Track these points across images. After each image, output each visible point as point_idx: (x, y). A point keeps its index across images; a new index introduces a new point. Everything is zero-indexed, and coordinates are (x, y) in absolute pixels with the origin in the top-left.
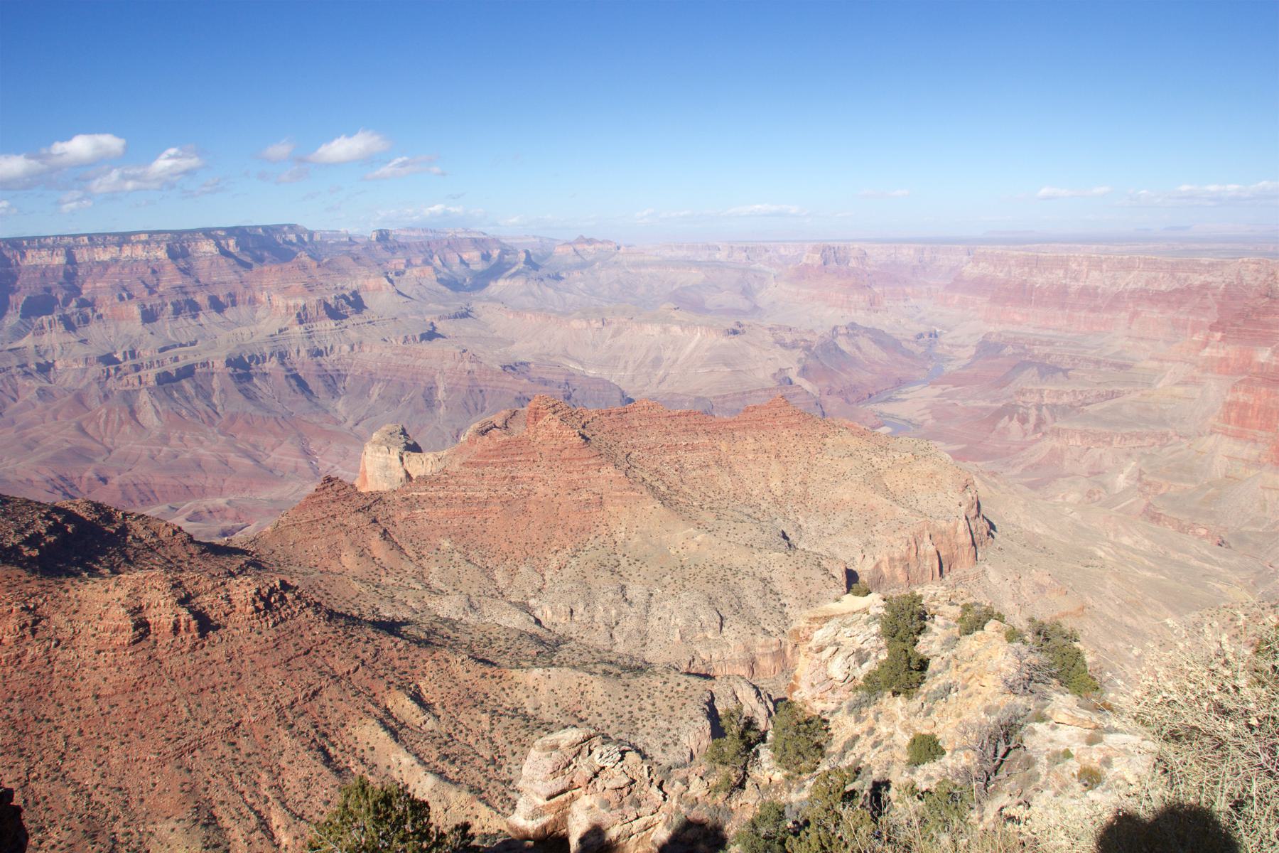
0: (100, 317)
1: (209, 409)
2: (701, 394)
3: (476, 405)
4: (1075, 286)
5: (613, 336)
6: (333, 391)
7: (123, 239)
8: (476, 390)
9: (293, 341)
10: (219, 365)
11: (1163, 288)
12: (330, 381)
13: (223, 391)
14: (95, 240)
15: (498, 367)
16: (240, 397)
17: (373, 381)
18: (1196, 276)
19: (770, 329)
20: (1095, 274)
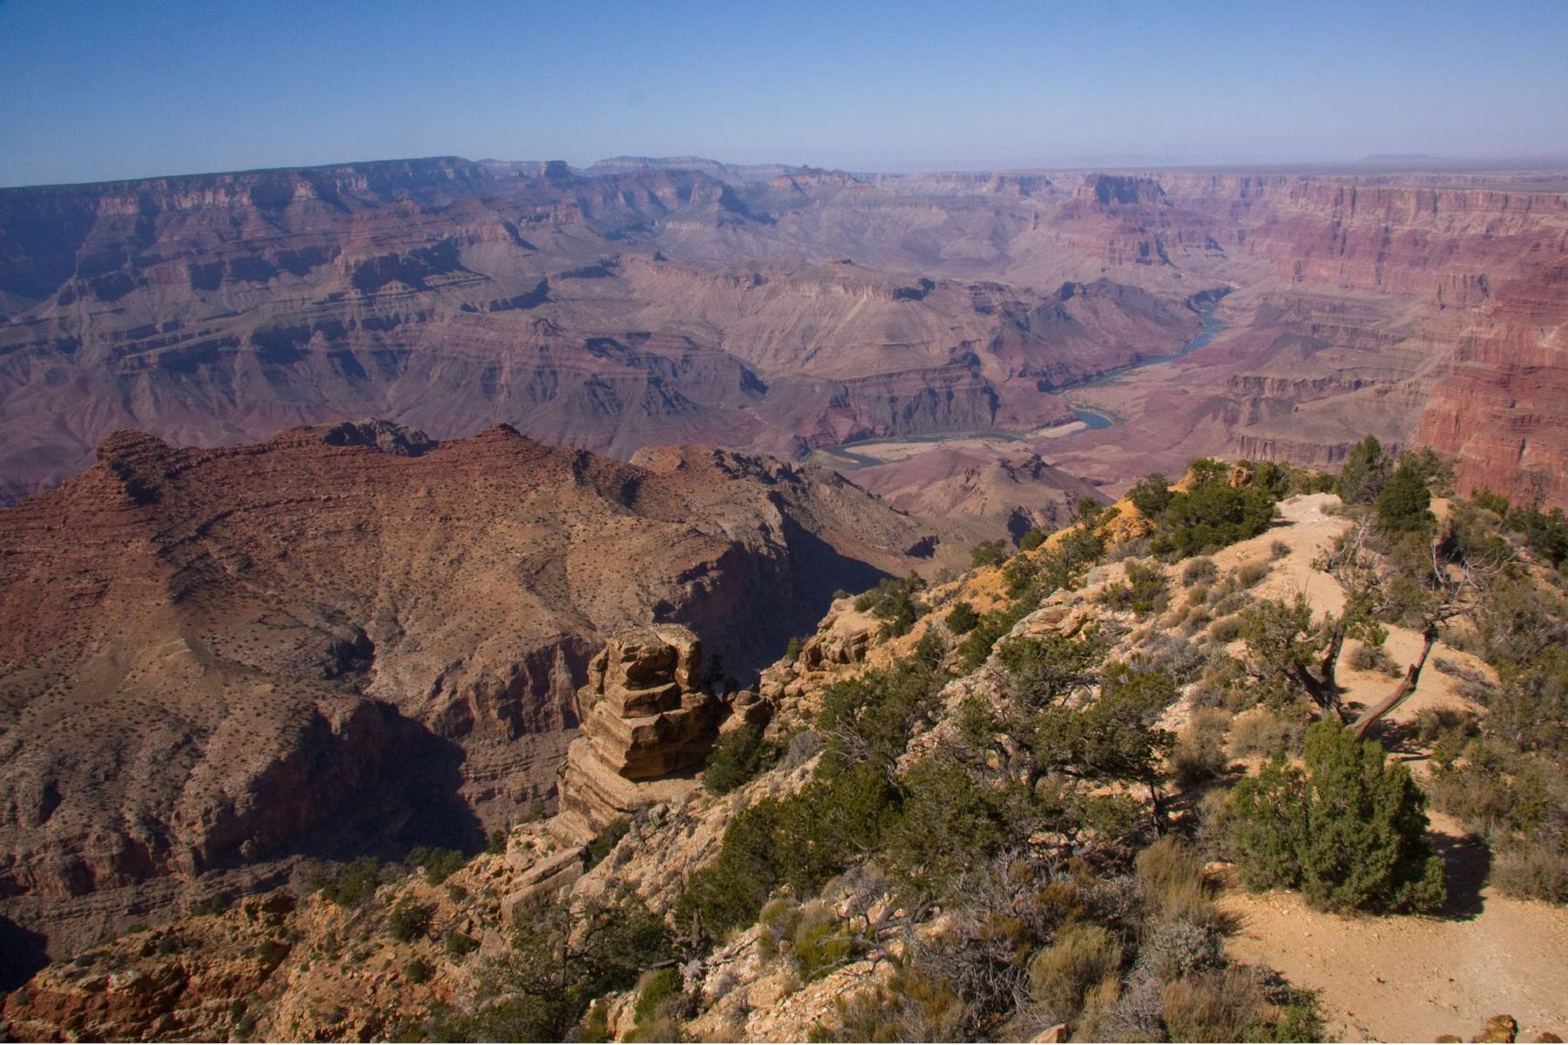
0: (144, 282)
1: (224, 399)
2: (834, 378)
3: (545, 390)
4: (1400, 230)
5: (768, 298)
6: (390, 374)
7: (208, 182)
8: (547, 370)
9: (348, 309)
10: (245, 340)
11: (1512, 233)
12: (388, 360)
13: (245, 373)
14: (177, 184)
15: (581, 341)
16: (260, 382)
17: (435, 358)
18: (318, 291)
19: (972, 288)
20: (1425, 214)
